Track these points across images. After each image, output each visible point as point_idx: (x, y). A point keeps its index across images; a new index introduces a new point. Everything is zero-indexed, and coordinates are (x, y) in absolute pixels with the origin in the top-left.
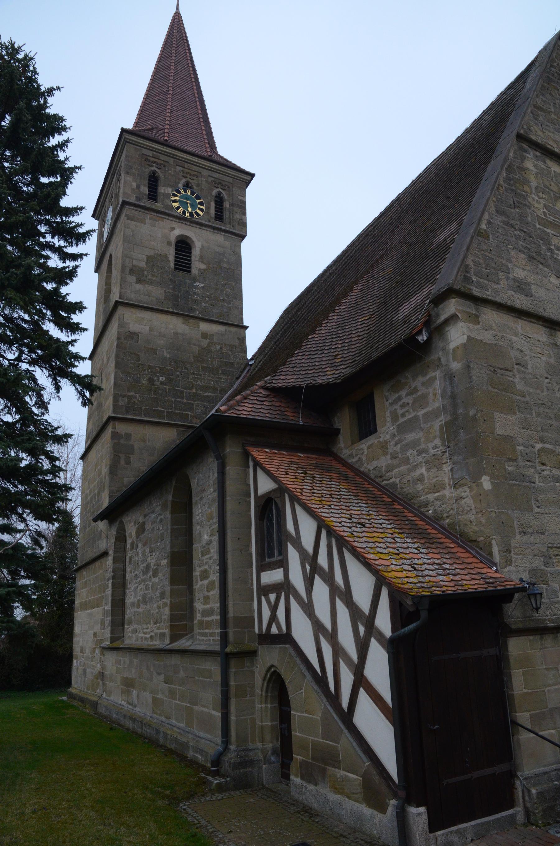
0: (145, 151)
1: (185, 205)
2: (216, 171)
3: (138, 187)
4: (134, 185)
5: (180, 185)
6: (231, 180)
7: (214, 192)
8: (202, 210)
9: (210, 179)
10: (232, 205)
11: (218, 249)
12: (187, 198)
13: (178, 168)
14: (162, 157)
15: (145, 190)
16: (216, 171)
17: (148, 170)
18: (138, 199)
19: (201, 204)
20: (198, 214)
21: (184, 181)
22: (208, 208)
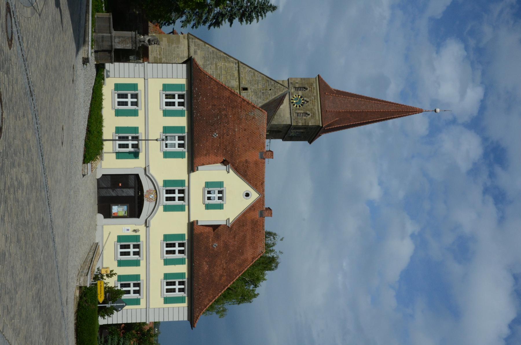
0: (314, 85)
1: (296, 99)
2: (318, 112)
3: (297, 83)
4: (297, 81)
5: (305, 99)
6: (317, 118)
7: (308, 112)
8: (297, 106)
9: (314, 110)
10: (305, 119)
11: (282, 115)
12: (300, 101)
13: (313, 97)
14: (315, 91)
15: (297, 86)
16: (318, 112)
17: (306, 86)
18: (291, 83)
19: (299, 106)
20: (294, 105)
21: (308, 100)
22: (299, 109)
